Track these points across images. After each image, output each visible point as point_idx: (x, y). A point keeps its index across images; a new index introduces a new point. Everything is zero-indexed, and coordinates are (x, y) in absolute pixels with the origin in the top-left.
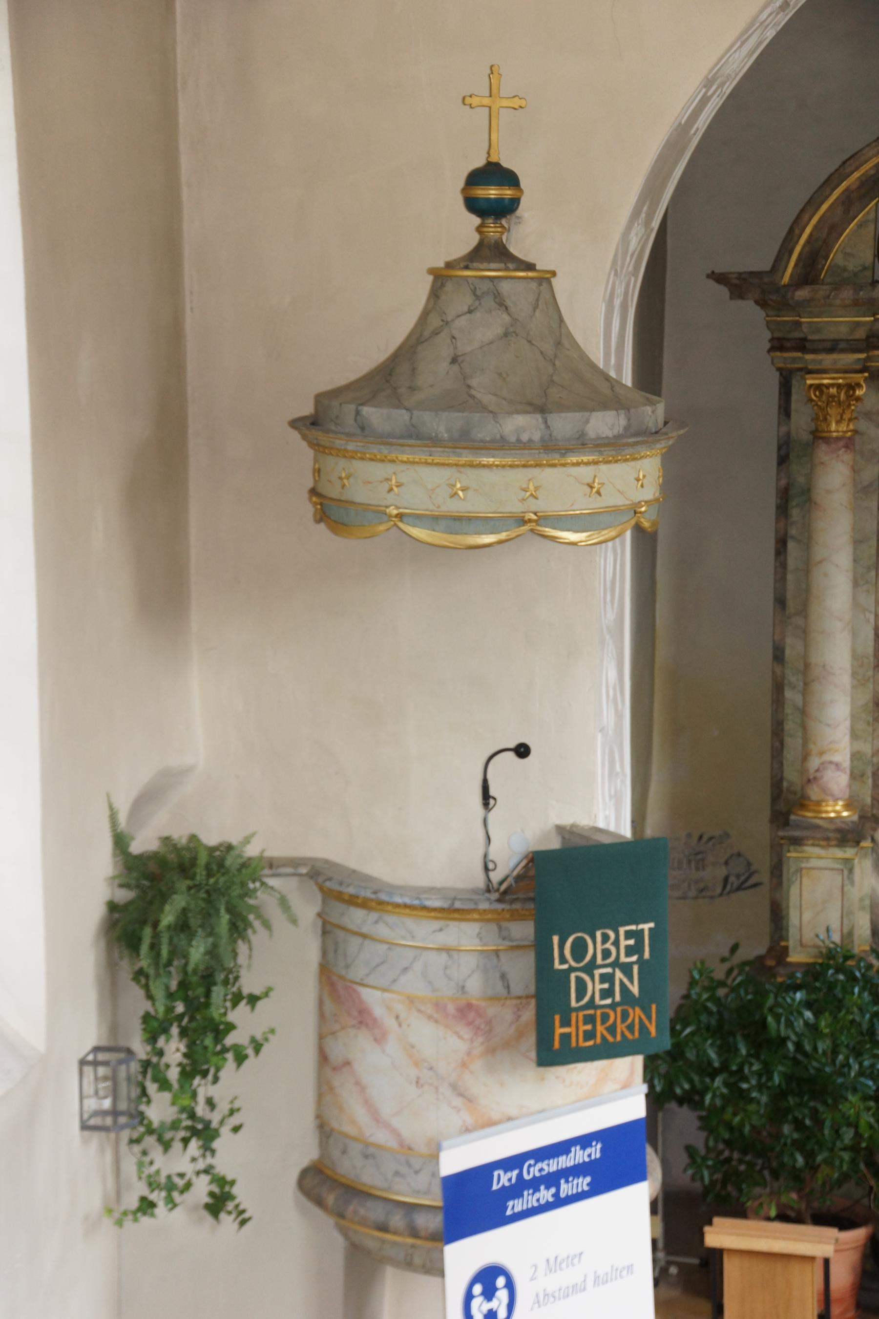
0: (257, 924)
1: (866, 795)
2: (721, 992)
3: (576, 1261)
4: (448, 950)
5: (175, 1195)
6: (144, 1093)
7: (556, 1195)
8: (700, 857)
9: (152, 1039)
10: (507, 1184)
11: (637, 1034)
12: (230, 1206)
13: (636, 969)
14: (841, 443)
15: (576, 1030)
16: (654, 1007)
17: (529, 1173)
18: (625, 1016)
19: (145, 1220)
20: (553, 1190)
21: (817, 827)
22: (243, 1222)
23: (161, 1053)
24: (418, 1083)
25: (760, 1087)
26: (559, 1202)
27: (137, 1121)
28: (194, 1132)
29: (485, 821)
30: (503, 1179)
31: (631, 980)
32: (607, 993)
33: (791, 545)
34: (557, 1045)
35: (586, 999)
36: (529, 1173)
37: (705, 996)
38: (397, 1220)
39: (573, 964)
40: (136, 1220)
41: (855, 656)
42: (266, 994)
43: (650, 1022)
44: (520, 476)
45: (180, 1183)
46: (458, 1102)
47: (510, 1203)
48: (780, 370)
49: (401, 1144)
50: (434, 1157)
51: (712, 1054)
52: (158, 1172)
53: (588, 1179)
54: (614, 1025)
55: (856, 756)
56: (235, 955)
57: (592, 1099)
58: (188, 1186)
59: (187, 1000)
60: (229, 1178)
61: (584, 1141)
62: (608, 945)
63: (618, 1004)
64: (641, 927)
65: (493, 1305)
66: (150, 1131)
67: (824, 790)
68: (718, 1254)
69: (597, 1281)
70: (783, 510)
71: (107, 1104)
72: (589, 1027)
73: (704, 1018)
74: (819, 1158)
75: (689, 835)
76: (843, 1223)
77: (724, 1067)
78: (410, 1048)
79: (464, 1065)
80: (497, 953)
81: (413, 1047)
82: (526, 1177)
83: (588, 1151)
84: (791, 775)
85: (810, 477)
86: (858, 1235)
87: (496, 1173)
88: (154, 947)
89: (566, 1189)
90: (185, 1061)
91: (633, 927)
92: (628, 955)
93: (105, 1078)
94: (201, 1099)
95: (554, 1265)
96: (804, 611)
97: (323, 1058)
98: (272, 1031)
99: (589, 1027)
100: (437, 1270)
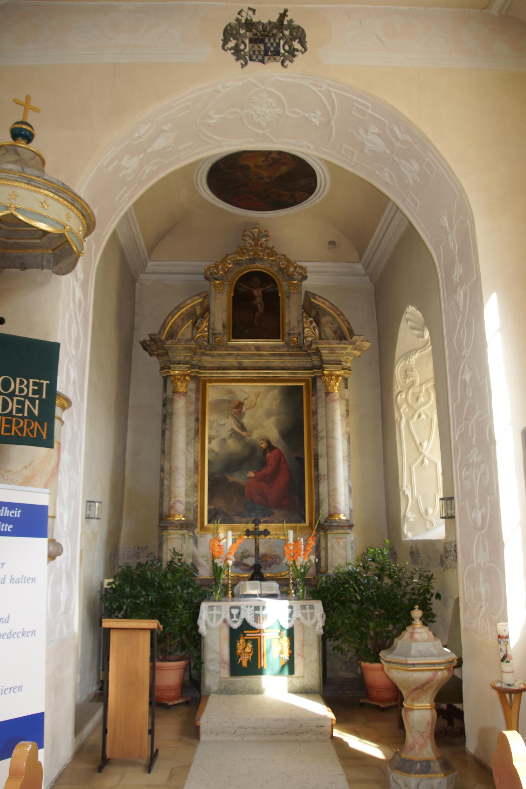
1: (191, 517)
8: (138, 554)
11: (35, 436)
13: (37, 402)
14: (182, 394)
16: (46, 424)
18: (29, 424)
21: (173, 523)
32: (19, 411)
33: (167, 432)
41: (187, 468)
43: (43, 432)
48: (164, 377)
53: (11, 526)
54: (23, 427)
55: (187, 503)
61: (12, 506)
62: (22, 386)
63: (26, 418)
64: (42, 381)
67: (176, 511)
68: (108, 631)
69: (12, 580)
70: (164, 421)
75: (135, 547)
84: (165, 510)
85: (172, 409)
91: (38, 381)
92: (33, 394)
96: (170, 454)
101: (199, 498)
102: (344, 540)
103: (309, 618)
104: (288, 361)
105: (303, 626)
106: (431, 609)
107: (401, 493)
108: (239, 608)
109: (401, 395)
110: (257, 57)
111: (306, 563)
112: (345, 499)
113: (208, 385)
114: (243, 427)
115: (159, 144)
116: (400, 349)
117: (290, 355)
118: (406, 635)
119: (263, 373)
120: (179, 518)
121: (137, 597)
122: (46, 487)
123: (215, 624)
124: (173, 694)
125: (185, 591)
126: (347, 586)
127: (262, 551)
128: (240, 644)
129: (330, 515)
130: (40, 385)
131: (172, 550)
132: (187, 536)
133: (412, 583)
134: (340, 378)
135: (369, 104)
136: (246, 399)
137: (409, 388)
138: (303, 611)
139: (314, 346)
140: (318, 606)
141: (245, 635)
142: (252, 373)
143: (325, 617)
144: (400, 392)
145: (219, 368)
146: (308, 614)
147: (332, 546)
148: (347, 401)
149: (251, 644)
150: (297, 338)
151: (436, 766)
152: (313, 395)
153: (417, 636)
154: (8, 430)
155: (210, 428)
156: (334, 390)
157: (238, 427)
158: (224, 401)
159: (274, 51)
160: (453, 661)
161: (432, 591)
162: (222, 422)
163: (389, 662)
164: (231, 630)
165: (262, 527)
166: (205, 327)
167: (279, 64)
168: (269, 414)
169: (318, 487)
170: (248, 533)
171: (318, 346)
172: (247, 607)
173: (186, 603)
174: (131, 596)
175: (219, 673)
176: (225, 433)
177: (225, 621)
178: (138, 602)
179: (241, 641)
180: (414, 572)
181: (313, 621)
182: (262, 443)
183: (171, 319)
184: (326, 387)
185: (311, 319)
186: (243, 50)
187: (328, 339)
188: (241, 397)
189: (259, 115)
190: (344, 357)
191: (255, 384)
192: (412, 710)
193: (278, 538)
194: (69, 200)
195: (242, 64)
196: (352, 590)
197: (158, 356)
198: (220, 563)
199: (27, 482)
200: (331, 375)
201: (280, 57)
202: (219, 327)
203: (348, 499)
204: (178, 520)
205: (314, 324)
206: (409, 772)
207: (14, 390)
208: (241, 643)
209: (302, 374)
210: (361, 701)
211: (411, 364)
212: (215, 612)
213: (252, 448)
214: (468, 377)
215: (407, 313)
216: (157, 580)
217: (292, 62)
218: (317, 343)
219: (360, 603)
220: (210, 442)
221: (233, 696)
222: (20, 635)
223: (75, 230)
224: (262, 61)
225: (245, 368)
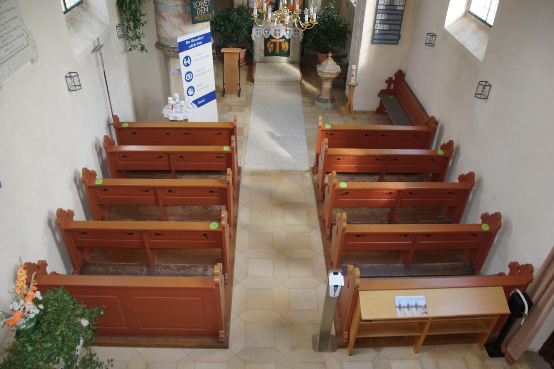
0: (143, 2)
2: (223, 13)
4: (176, 5)
5: (135, 48)
6: (128, 31)
7: (197, 45)
9: (128, 22)
12: (144, 49)
13: (207, 7)
15: (198, 18)
16: (211, 14)
18: (206, 15)
19: (131, 52)
20: (196, 44)
22: (147, 52)
23: (130, 25)
24: (173, 28)
25: (230, 28)
26: (197, 46)
27: (127, 36)
28: (137, 38)
30: (188, 43)
31: (207, 9)
32: (203, 11)
34: (195, 20)
35: (199, 13)
37: (221, 14)
38: (172, 50)
39: (197, 7)
40: (129, 52)
42: (146, 14)
45: (136, 46)
46: (180, 30)
49: (171, 38)
50: (176, 40)
51: (222, 23)
52: (132, 44)
53: (202, 42)
54: (204, 17)
56: (140, 7)
57: (202, 29)
58: (137, 46)
59: (133, 16)
60: (144, 44)
61: (201, 36)
65: (188, 62)
66: (130, 38)
68: (223, 53)
69: (204, 57)
71: (122, 33)
72: (200, 17)
73: (221, 17)
74: (239, 39)
76: (242, 49)
77: (224, 25)
78: (171, 22)
79: (180, 25)
80: (184, 5)
81: (171, 22)
82: (192, 42)
86: (245, 50)
87: (187, 42)
88: (126, 6)
89: (198, 44)
90: (134, 26)
93: (121, 29)
94: (137, 32)
95: (197, 55)
97: (157, 25)
98: (148, 20)
99: (200, 17)
100: (178, 57)
103: (297, 35)
105: (294, 39)
123: (259, 36)
138: (295, 32)
141: (270, 41)
146: (297, 34)
149: (273, 44)
151: (329, 101)
164: (265, 39)
175: (260, 55)
177: (263, 35)
179: (269, 43)
181: (299, 36)
192: (324, 84)
207: (200, 6)
208: (269, 44)
212: (259, 32)
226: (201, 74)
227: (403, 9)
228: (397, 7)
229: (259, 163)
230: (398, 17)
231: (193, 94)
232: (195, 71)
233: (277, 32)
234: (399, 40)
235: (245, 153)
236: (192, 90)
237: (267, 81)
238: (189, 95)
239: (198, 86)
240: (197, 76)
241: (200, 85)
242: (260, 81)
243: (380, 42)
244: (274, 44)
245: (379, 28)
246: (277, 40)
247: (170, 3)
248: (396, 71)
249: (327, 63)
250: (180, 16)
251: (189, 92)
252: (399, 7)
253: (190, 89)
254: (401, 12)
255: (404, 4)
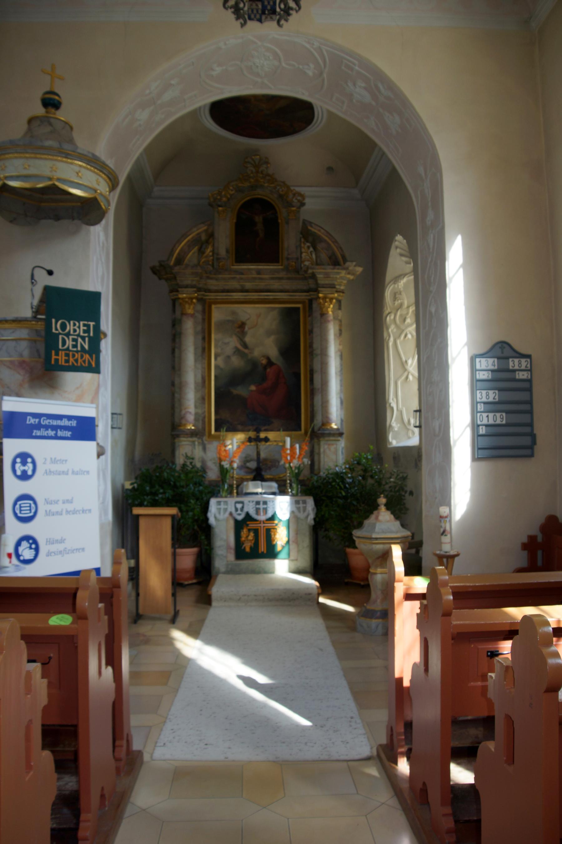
3: (64, 462)
7: (56, 434)
10: (33, 423)
11: (87, 365)
13: (87, 339)
15: (62, 358)
17: (44, 422)
18: (82, 357)
20: (54, 432)
26: (56, 437)
29: (32, 290)
30: (31, 421)
31: (85, 342)
32: (75, 346)
33: (177, 350)
34: (53, 362)
35: (66, 347)
36: (44, 422)
39: (61, 331)
44: (49, 164)
47: (35, 431)
53: (70, 433)
55: (196, 414)
61: (70, 418)
62: (76, 327)
64: (89, 323)
65: (26, 468)
68: (138, 516)
69: (73, 472)
70: (174, 340)
79: (21, 385)
80: (35, 341)
83: (70, 422)
84: (177, 420)
87: (28, 417)
89: (60, 433)
91: (86, 323)
95: (54, 461)
96: (180, 369)
101: (206, 410)
102: (335, 446)
104: (286, 284)
106: (404, 504)
107: (388, 405)
108: (242, 503)
109: (390, 317)
110: (255, 16)
111: (300, 465)
112: (337, 411)
113: (213, 306)
114: (245, 346)
115: (167, 96)
116: (390, 274)
117: (289, 279)
118: (373, 517)
119: (264, 295)
120: (191, 427)
121: (156, 494)
122: (92, 402)
123: (223, 516)
124: (188, 575)
125: (196, 489)
126: (334, 484)
127: (263, 455)
128: (244, 534)
129: (323, 424)
130: (88, 326)
131: (185, 455)
132: (196, 443)
133: (390, 482)
134: (334, 301)
135: (356, 62)
136: (248, 319)
137: (397, 310)
138: (298, 506)
139: (310, 271)
140: (310, 502)
141: (247, 525)
142: (253, 296)
143: (315, 510)
144: (389, 313)
145: (223, 291)
147: (324, 451)
148: (340, 321)
149: (254, 533)
150: (295, 263)
152: (309, 316)
153: (381, 518)
154: (67, 361)
155: (216, 346)
156: (328, 312)
157: (241, 345)
158: (229, 321)
159: (271, 10)
160: (407, 537)
161: (406, 489)
162: (227, 340)
163: (359, 537)
164: (236, 521)
165: (262, 435)
166: (210, 252)
167: (275, 23)
168: (269, 333)
169: (312, 399)
170: (250, 440)
171: (314, 271)
172: (249, 502)
173: (197, 499)
174: (151, 493)
175: (226, 557)
176: (229, 350)
177: (231, 514)
178: (157, 498)
180: (393, 473)
181: (306, 514)
182: (262, 360)
183: (178, 247)
184: (321, 309)
185: (308, 244)
186: (242, 9)
187: (323, 265)
188: (243, 317)
189: (257, 67)
190: (339, 281)
191: (257, 306)
192: (376, 574)
193: (277, 445)
194: (99, 168)
195: (241, 24)
196: (338, 487)
197: (167, 280)
198: (226, 464)
199: (79, 399)
200: (324, 298)
201: (277, 15)
202: (222, 252)
203: (339, 410)
204: (188, 429)
205: (311, 249)
206: (371, 618)
207: (70, 331)
208: (244, 532)
209: (299, 296)
210: (346, 580)
211: (400, 287)
212: (222, 506)
213: (254, 364)
214: (433, 310)
215: (396, 241)
216: (172, 479)
217: (286, 20)
218: (313, 269)
219: (345, 498)
220: (216, 359)
221: (237, 577)
222: (81, 512)
223: (104, 192)
224: (260, 21)
225: (247, 291)
226: (62, 511)
227: (529, 377)
228: (517, 373)
229: (206, 744)
230: (523, 396)
231: (32, 558)
232: (46, 499)
233: (261, 506)
234: (535, 447)
235: (165, 722)
236: (31, 548)
237: (239, 600)
238: (22, 558)
239: (50, 542)
240: (48, 513)
241: (57, 542)
242: (225, 601)
243: (494, 452)
244: (256, 532)
245: (485, 421)
246: (260, 523)
247: (3, 336)
248: (542, 520)
249: (377, 518)
250: (22, 364)
251: (20, 549)
252: (521, 373)
253: (25, 544)
254: (526, 385)
255: (529, 366)
